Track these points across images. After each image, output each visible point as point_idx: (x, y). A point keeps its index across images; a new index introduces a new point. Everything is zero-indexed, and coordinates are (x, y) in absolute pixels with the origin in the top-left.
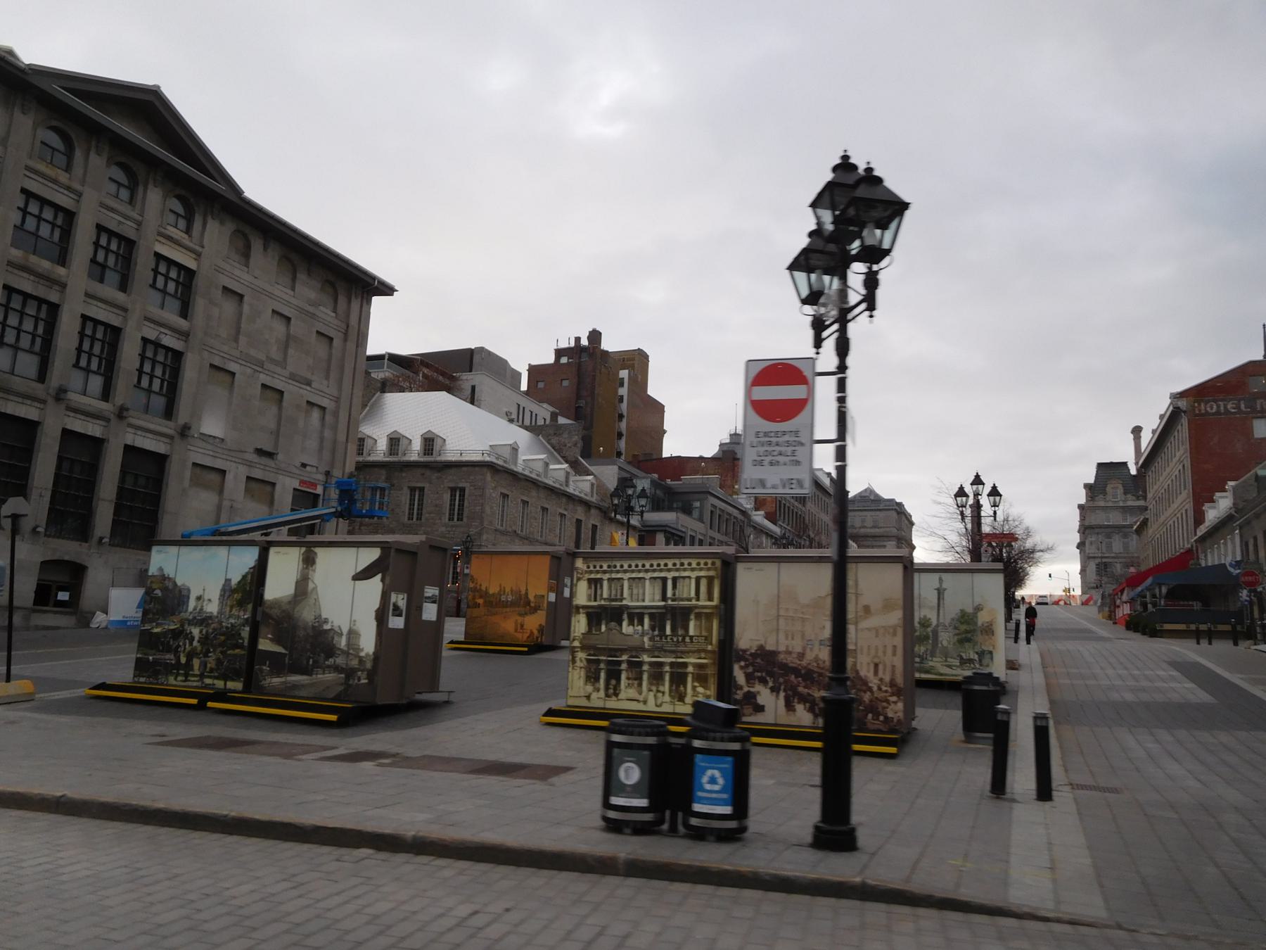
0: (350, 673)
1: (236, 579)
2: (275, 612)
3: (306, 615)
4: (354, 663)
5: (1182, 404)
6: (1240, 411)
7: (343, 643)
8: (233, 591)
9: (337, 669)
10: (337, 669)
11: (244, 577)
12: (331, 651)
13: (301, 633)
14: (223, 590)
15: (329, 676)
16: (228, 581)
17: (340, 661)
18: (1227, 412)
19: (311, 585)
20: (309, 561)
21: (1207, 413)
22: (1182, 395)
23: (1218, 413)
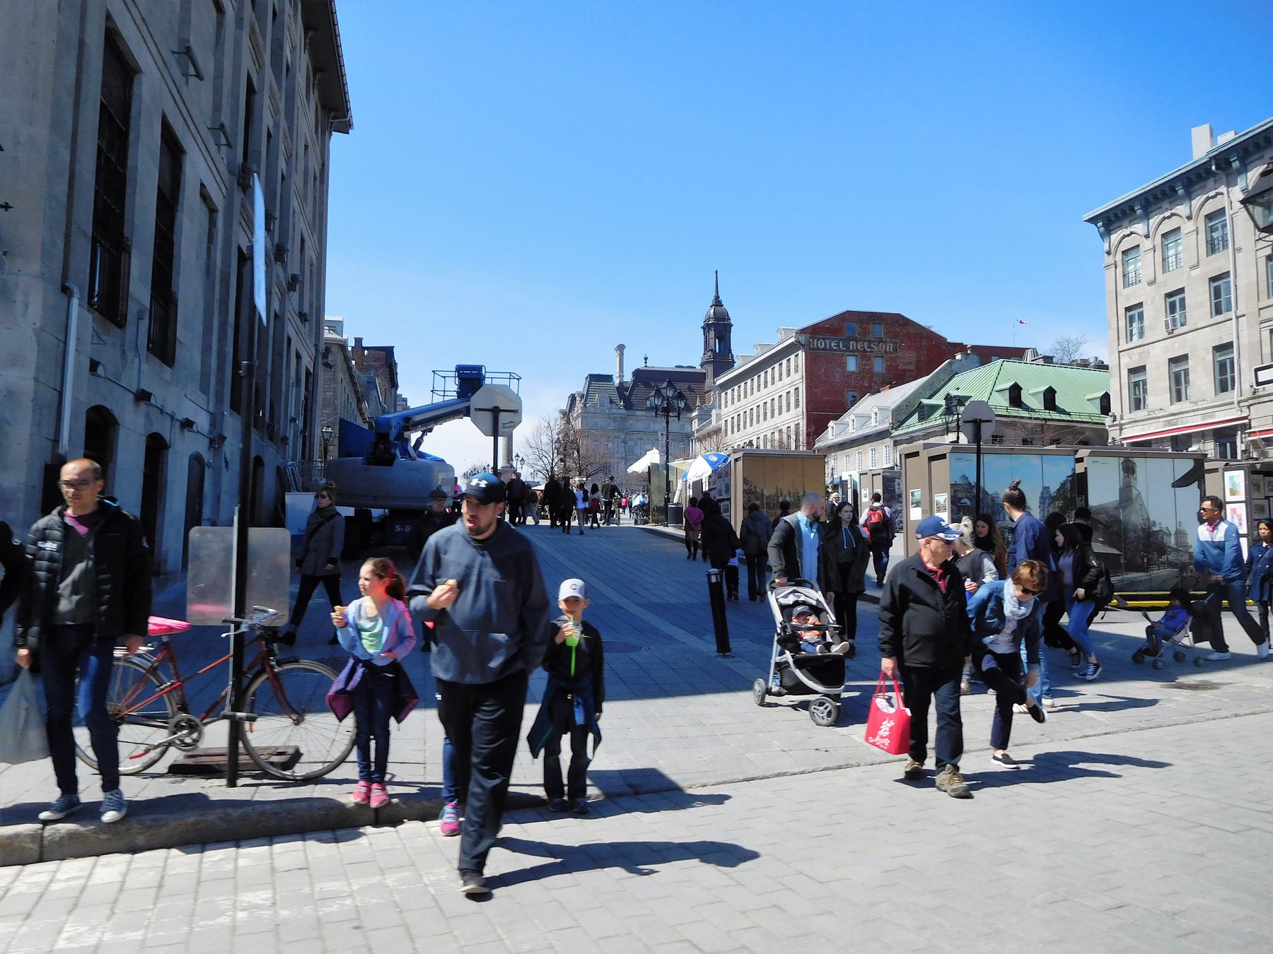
0: (1183, 567)
1: (1054, 488)
2: (1103, 518)
3: (1134, 519)
4: (1186, 558)
5: (802, 339)
6: (839, 350)
7: (1172, 542)
8: (1053, 499)
9: (1171, 564)
10: (1171, 564)
11: (1063, 485)
12: (1163, 549)
13: (1132, 535)
14: (1042, 498)
15: (1165, 572)
16: (1046, 489)
17: (1172, 557)
18: (831, 349)
19: (1134, 492)
20: (1129, 469)
21: (818, 349)
22: (803, 331)
23: (825, 349)
